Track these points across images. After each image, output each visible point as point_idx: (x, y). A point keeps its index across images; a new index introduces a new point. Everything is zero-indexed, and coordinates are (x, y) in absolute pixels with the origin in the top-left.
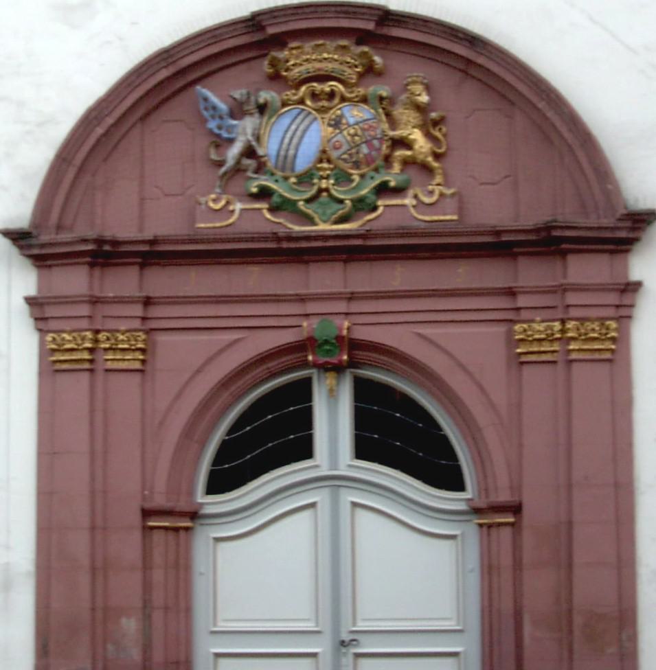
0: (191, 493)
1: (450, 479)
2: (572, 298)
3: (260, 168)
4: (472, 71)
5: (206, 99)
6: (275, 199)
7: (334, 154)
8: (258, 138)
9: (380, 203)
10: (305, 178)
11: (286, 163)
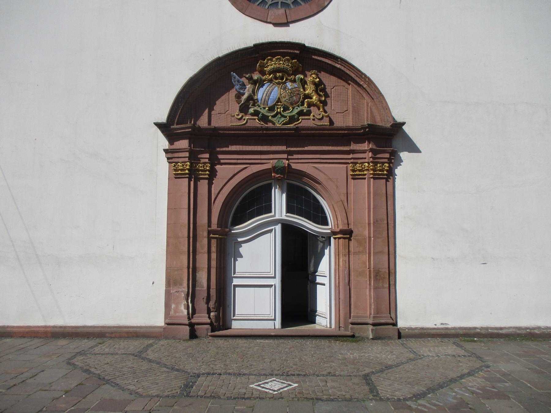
3: (255, 104)
10: (271, 109)
11: (265, 102)
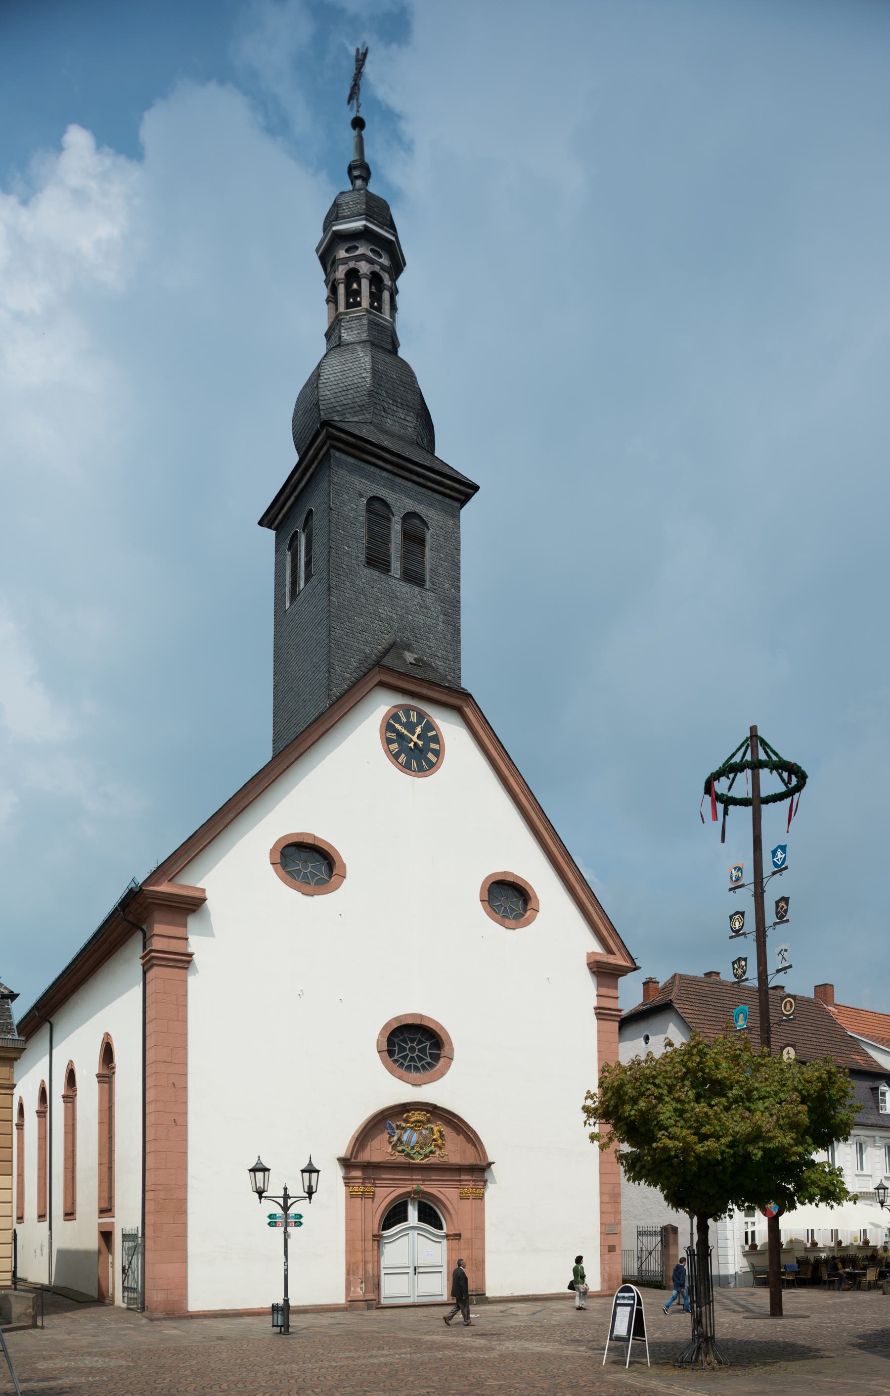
3: (402, 1143)
4: (451, 1123)
10: (413, 1148)
11: (408, 1142)
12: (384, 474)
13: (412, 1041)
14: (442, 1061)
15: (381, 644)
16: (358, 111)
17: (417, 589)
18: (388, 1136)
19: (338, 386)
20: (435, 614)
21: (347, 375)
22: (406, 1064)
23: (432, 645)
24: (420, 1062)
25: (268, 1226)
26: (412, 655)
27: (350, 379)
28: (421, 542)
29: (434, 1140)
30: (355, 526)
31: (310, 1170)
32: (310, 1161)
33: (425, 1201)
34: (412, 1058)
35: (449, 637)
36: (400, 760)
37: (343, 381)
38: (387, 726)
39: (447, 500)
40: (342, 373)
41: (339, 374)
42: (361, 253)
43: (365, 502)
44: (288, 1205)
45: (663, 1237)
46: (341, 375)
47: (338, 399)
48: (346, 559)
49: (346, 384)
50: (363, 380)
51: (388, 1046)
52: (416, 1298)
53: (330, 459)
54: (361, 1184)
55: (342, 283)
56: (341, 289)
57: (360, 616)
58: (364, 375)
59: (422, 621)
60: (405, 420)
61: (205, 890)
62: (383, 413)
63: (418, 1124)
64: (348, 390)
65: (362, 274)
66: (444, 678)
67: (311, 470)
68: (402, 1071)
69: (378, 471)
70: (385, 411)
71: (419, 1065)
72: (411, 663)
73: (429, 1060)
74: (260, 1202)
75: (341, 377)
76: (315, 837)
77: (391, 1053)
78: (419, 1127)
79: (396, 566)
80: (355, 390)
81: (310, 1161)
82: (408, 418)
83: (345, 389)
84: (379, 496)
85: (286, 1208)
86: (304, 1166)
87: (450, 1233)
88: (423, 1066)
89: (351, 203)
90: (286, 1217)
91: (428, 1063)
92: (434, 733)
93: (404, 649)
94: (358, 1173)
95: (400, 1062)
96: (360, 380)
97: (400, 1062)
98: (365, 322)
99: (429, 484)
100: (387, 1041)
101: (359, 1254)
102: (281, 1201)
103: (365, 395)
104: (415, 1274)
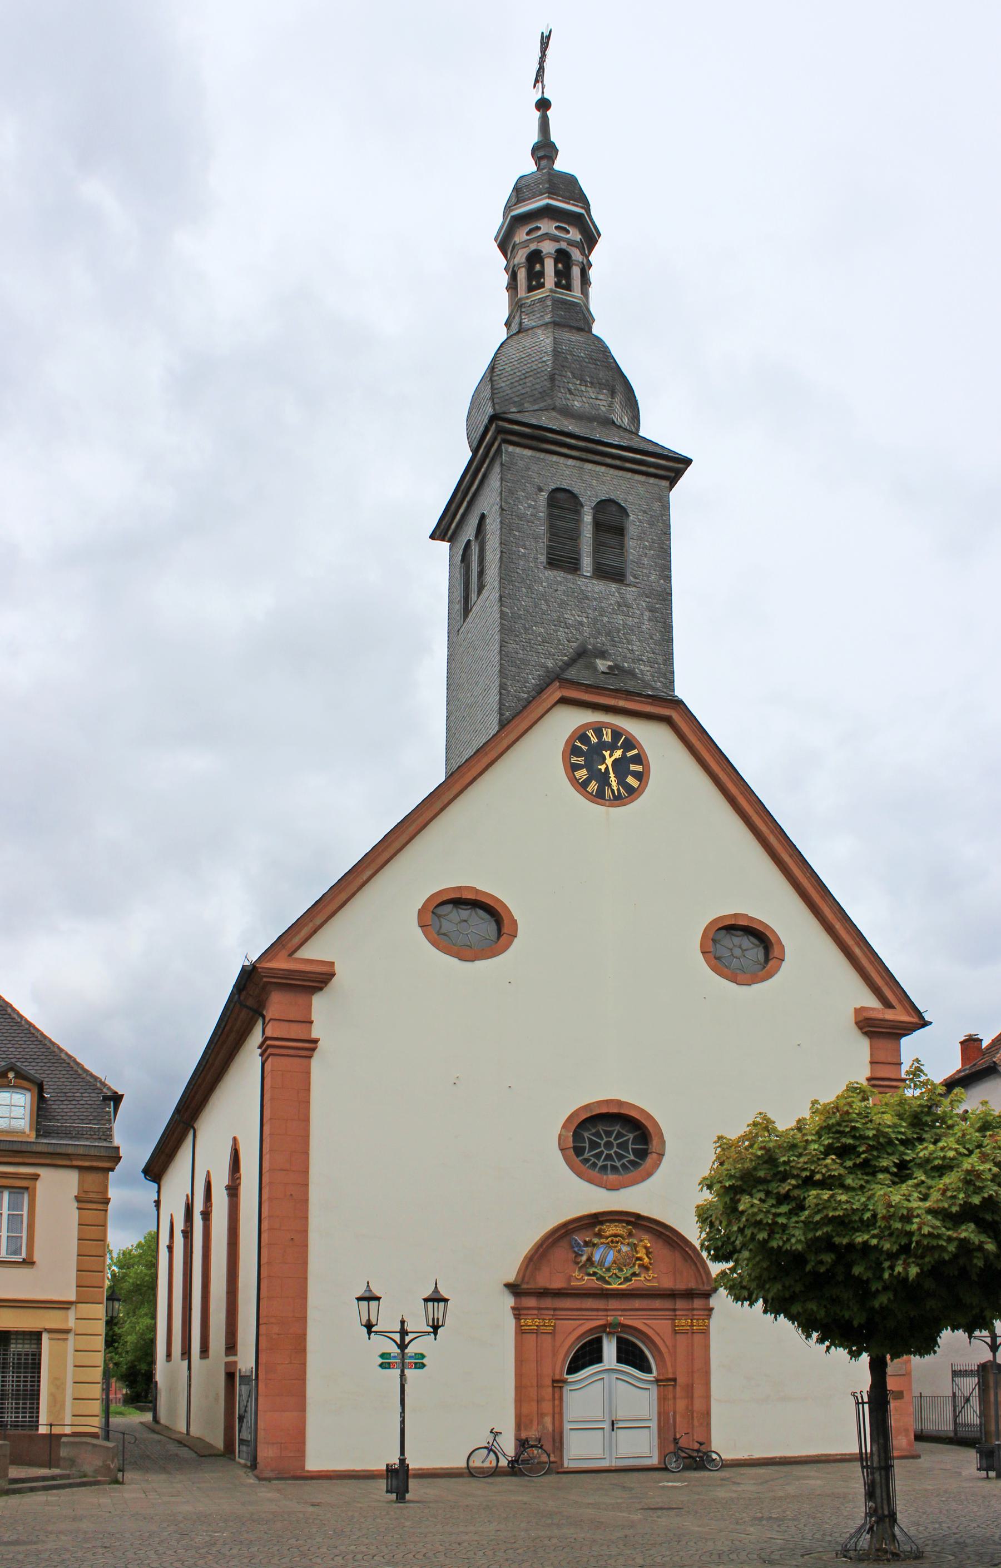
0: (561, 1374)
1: (648, 1370)
2: (695, 1312)
5: (576, 1240)
6: (598, 1275)
7: (618, 1262)
8: (592, 1254)
9: (633, 1278)
10: (608, 1270)
11: (601, 1264)
12: (570, 462)
13: (608, 1134)
14: (650, 1160)
15: (567, 654)
16: (543, 93)
17: (614, 587)
18: (574, 1255)
19: (514, 376)
20: (638, 612)
21: (525, 363)
22: (600, 1164)
23: (635, 648)
24: (619, 1160)
25: (380, 1369)
26: (604, 662)
27: (529, 365)
28: (620, 531)
29: (638, 1259)
30: (533, 525)
31: (436, 1298)
32: (436, 1287)
33: (625, 1336)
34: (609, 1157)
35: (657, 636)
36: (589, 789)
37: (520, 369)
38: (572, 749)
39: (652, 480)
40: (519, 361)
41: (515, 363)
42: (545, 232)
43: (546, 497)
44: (406, 1343)
45: (981, 1378)
46: (519, 363)
47: (514, 390)
48: (522, 563)
49: (524, 372)
50: (544, 364)
51: (574, 1142)
52: (614, 1460)
53: (502, 455)
54: (535, 1317)
55: (523, 267)
56: (522, 275)
57: (540, 625)
58: (544, 359)
59: (621, 623)
60: (597, 399)
61: (334, 963)
62: (568, 396)
63: (615, 1239)
64: (526, 378)
65: (546, 254)
66: (647, 685)
67: (483, 470)
68: (594, 1173)
69: (562, 460)
70: (571, 393)
71: (618, 1164)
72: (603, 673)
73: (632, 1157)
74: (369, 1339)
75: (518, 366)
76: (477, 891)
77: (578, 1151)
78: (617, 1242)
79: (587, 563)
80: (535, 377)
81: (436, 1287)
82: (601, 397)
83: (523, 377)
84: (563, 487)
85: (402, 1346)
86: (428, 1293)
87: (661, 1377)
88: (623, 1166)
89: (533, 185)
90: (403, 1356)
91: (631, 1162)
92: (635, 752)
93: (596, 657)
94: (531, 1302)
95: (591, 1162)
96: (540, 365)
97: (591, 1162)
98: (549, 303)
99: (628, 465)
100: (573, 1135)
101: (534, 1404)
102: (397, 1337)
103: (546, 380)
104: (613, 1430)
